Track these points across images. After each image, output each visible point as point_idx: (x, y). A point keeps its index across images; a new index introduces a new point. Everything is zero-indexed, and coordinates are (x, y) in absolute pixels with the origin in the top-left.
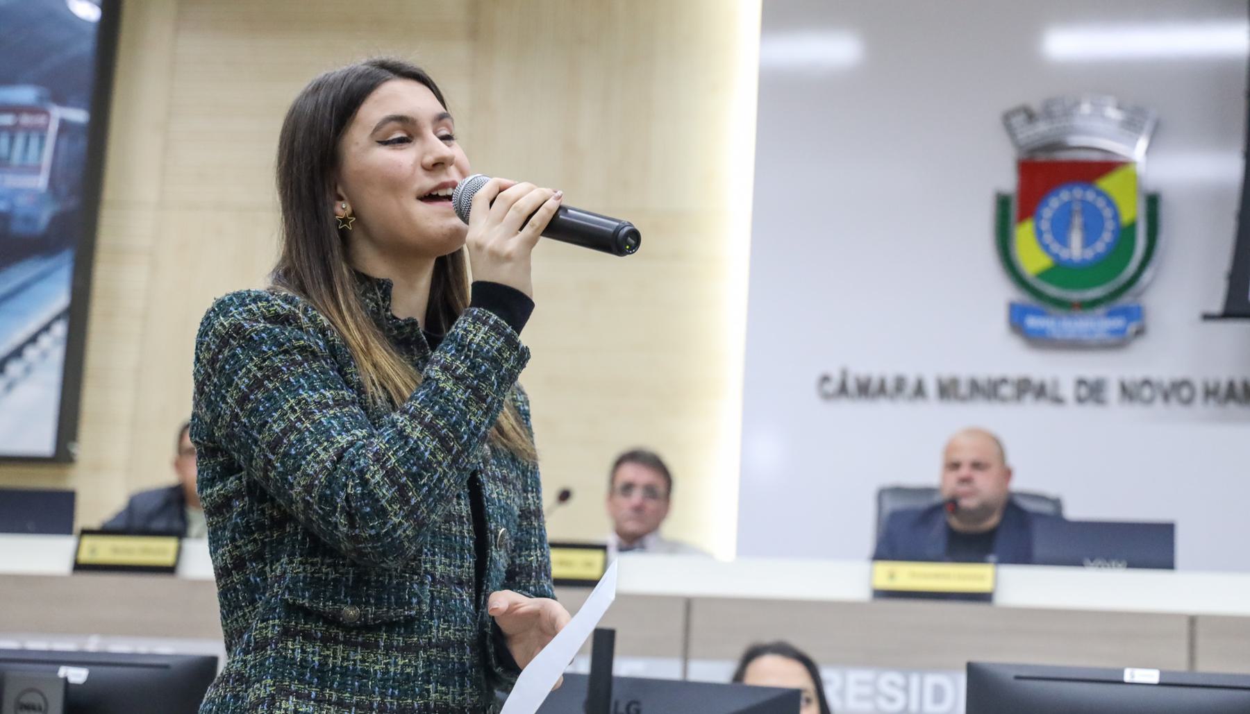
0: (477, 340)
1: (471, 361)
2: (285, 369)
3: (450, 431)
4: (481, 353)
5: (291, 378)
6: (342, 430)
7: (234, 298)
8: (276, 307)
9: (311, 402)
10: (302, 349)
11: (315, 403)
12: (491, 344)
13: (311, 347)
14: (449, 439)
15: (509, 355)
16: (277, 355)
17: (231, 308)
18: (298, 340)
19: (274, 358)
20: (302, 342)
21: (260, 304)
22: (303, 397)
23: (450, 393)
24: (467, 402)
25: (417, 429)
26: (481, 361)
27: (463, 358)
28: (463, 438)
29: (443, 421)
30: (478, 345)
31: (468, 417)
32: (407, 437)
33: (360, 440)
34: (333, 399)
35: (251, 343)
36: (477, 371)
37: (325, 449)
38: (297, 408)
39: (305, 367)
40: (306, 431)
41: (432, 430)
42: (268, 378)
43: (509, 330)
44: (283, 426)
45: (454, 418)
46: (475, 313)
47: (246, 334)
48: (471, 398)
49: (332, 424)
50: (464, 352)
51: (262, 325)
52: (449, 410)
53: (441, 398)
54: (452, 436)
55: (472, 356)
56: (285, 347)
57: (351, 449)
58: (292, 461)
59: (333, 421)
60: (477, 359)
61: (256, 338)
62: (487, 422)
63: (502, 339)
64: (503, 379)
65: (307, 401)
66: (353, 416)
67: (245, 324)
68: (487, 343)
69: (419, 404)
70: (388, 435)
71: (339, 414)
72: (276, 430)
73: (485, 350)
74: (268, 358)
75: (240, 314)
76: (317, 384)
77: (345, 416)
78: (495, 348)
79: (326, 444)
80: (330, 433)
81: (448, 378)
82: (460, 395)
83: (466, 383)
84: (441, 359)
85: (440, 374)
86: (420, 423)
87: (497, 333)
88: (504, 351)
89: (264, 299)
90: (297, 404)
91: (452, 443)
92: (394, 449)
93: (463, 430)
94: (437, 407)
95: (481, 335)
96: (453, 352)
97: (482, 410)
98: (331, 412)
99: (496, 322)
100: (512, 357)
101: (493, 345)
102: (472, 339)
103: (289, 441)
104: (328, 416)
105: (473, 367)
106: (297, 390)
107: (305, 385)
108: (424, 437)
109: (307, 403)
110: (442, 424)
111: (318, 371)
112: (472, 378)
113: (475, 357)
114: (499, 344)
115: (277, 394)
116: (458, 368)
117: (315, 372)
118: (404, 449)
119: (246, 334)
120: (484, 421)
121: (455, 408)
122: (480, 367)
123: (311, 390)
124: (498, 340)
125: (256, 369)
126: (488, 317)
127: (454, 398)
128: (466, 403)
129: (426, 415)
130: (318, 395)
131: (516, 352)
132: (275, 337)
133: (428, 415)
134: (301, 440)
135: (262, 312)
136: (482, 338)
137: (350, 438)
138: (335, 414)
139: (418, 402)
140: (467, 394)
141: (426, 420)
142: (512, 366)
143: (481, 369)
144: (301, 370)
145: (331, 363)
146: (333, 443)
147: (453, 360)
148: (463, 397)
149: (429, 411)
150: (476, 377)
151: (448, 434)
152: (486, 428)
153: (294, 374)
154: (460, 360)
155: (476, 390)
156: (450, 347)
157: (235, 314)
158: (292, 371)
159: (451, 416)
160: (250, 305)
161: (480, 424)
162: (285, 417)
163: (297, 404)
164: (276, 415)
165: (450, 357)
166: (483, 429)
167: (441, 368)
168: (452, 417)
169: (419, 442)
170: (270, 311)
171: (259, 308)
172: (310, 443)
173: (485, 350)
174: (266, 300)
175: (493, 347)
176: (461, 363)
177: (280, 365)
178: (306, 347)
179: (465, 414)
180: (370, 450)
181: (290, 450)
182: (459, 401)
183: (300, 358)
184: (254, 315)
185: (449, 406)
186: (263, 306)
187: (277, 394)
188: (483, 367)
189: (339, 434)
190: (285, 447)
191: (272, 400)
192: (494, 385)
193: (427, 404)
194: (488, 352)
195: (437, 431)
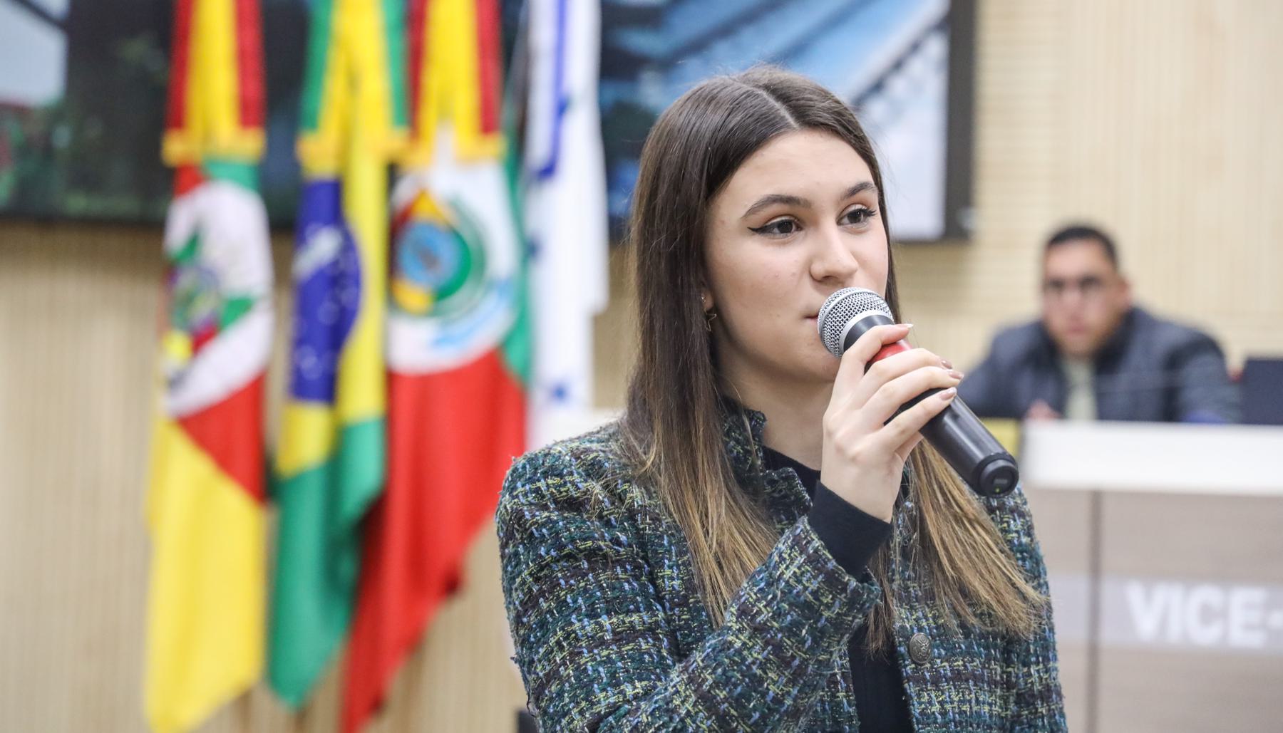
0: (788, 575)
1: (778, 603)
2: (562, 582)
3: (733, 708)
4: (789, 595)
5: (569, 596)
6: (609, 684)
7: (528, 466)
8: (569, 485)
9: (583, 636)
10: (591, 554)
11: (588, 638)
12: (804, 582)
13: (602, 550)
14: (731, 718)
15: (832, 599)
16: (558, 561)
17: (519, 484)
18: (585, 540)
19: (552, 564)
20: (590, 543)
21: (550, 482)
22: (573, 627)
23: (739, 652)
24: (765, 664)
25: (691, 700)
26: (787, 607)
27: (770, 596)
28: (752, 716)
29: (724, 692)
30: (787, 582)
31: (765, 685)
32: (674, 711)
33: (629, 702)
34: (613, 631)
35: (531, 541)
36: (783, 620)
37: (581, 713)
38: (565, 644)
39: (588, 580)
40: (567, 681)
41: (708, 704)
42: (542, 593)
43: (833, 564)
44: (548, 668)
45: (739, 689)
46: (798, 531)
47: (527, 527)
48: (770, 660)
49: (599, 672)
50: (772, 588)
51: (546, 514)
52: (732, 677)
53: (726, 658)
54: (735, 713)
55: (779, 598)
56: (567, 551)
57: (610, 718)
58: (550, 722)
59: (601, 669)
60: (783, 604)
61: (536, 534)
62: (795, 692)
63: (821, 577)
64: (823, 631)
65: (577, 634)
66: (638, 658)
67: (527, 513)
68: (799, 581)
69: (703, 661)
70: (656, 702)
71: (614, 656)
72: (541, 674)
73: (795, 591)
74: (547, 564)
75: (526, 495)
76: (600, 606)
77: (623, 658)
78: (810, 589)
79: (583, 704)
80: (593, 687)
81: (744, 627)
82: (757, 654)
83: (766, 636)
84: (744, 595)
85: (735, 619)
86: (695, 691)
87: (814, 568)
88: (823, 595)
89: (558, 472)
90: (565, 639)
91: (735, 724)
92: (656, 725)
93: (752, 704)
94: (720, 671)
95: (793, 569)
96: (762, 585)
97: (786, 677)
98: (605, 653)
99: (816, 551)
100: (837, 603)
101: (807, 585)
102: (782, 573)
103: (550, 691)
104: (599, 659)
105: (778, 615)
106: (570, 615)
107: (583, 607)
108: (697, 713)
109: (577, 639)
110: (722, 695)
111: (605, 585)
112: (777, 629)
113: (782, 601)
114: (813, 586)
115: (551, 620)
116: (759, 612)
117: (601, 588)
118: (668, 727)
119: (527, 527)
120: (788, 693)
121: (741, 676)
122: (786, 615)
123: (587, 616)
124: (815, 577)
125: (531, 580)
126: (808, 542)
127: (744, 659)
128: (762, 666)
129: (705, 680)
130: (593, 626)
131: (843, 595)
132: (557, 534)
133: (707, 680)
134: (560, 694)
135: (552, 493)
136: (795, 572)
137: (612, 700)
138: (608, 656)
139: (703, 656)
140: (766, 652)
141: (704, 687)
142: (838, 613)
143: (786, 618)
144: (582, 584)
145: (632, 570)
146: (592, 704)
147: (758, 600)
148: (760, 657)
149: (710, 674)
150: (781, 630)
151: (729, 711)
152: (795, 700)
153: (573, 590)
154: (766, 600)
155: (778, 648)
156: (761, 576)
157: (520, 494)
158: (571, 585)
159: (735, 686)
160: (539, 481)
161: (783, 695)
162: (551, 656)
163: (565, 639)
164: (542, 651)
165: (755, 594)
166: (788, 702)
167: (739, 609)
168: (736, 688)
169: (688, 721)
170: (561, 493)
171: (548, 486)
172: (567, 700)
173: (795, 591)
174: (557, 476)
175: (806, 588)
176: (765, 606)
177: (560, 575)
178: (594, 550)
179: (761, 681)
180: (630, 721)
181: (549, 707)
182: (754, 663)
183: (586, 565)
184: (543, 497)
185: (734, 670)
186: (553, 484)
187: (551, 620)
188: (789, 618)
189: (603, 690)
190: (547, 700)
191: (545, 627)
192: (805, 642)
193: (711, 663)
194: (798, 594)
195: (715, 706)
